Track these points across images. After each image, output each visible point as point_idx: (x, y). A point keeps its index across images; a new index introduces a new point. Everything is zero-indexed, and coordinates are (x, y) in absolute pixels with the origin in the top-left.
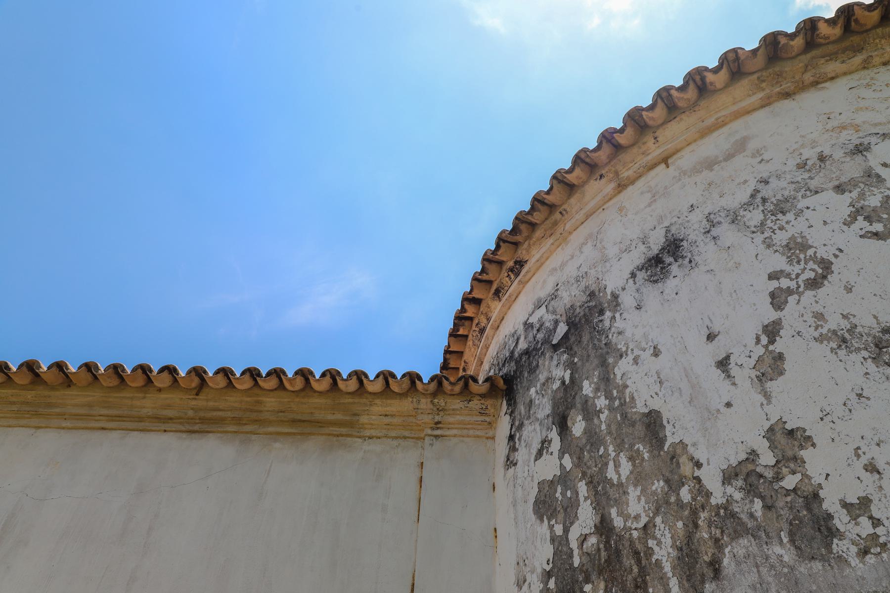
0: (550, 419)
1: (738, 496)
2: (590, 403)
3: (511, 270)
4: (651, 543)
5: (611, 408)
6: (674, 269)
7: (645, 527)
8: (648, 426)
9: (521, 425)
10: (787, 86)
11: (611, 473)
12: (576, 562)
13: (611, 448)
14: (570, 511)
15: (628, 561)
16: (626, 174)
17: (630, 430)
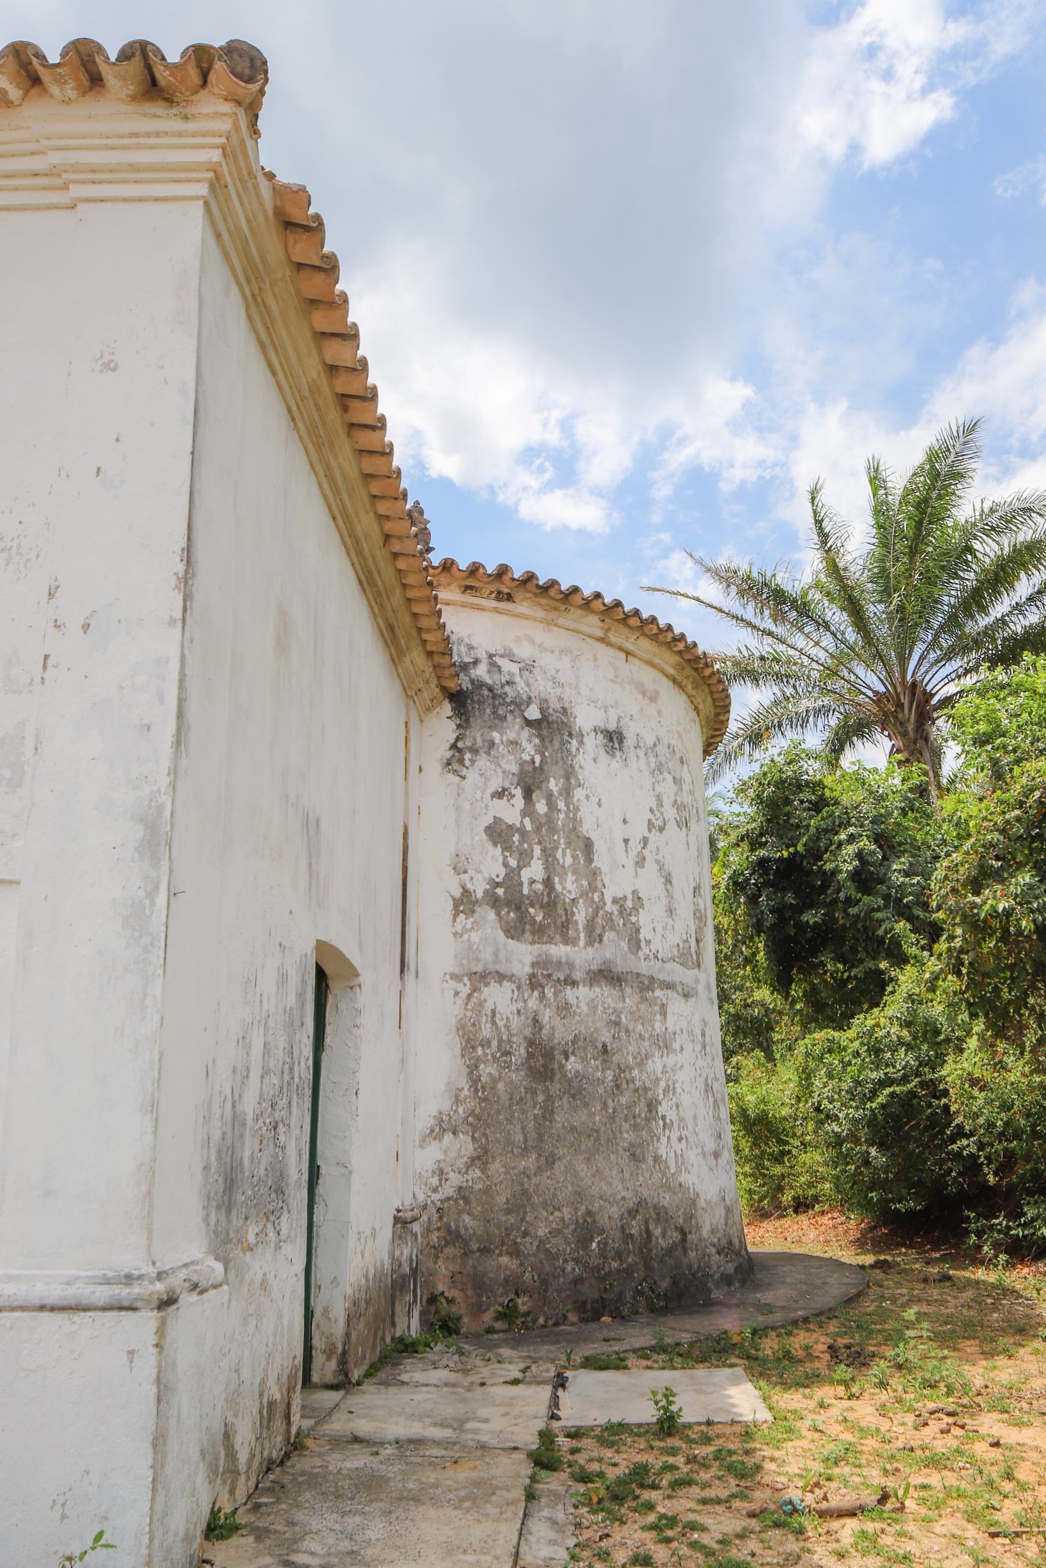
0: (515, 779)
1: (616, 913)
2: (554, 798)
6: (618, 753)
7: (573, 900)
8: (586, 846)
10: (679, 678)
11: (559, 854)
12: (526, 891)
13: (562, 841)
14: (524, 858)
15: (561, 912)
17: (576, 839)
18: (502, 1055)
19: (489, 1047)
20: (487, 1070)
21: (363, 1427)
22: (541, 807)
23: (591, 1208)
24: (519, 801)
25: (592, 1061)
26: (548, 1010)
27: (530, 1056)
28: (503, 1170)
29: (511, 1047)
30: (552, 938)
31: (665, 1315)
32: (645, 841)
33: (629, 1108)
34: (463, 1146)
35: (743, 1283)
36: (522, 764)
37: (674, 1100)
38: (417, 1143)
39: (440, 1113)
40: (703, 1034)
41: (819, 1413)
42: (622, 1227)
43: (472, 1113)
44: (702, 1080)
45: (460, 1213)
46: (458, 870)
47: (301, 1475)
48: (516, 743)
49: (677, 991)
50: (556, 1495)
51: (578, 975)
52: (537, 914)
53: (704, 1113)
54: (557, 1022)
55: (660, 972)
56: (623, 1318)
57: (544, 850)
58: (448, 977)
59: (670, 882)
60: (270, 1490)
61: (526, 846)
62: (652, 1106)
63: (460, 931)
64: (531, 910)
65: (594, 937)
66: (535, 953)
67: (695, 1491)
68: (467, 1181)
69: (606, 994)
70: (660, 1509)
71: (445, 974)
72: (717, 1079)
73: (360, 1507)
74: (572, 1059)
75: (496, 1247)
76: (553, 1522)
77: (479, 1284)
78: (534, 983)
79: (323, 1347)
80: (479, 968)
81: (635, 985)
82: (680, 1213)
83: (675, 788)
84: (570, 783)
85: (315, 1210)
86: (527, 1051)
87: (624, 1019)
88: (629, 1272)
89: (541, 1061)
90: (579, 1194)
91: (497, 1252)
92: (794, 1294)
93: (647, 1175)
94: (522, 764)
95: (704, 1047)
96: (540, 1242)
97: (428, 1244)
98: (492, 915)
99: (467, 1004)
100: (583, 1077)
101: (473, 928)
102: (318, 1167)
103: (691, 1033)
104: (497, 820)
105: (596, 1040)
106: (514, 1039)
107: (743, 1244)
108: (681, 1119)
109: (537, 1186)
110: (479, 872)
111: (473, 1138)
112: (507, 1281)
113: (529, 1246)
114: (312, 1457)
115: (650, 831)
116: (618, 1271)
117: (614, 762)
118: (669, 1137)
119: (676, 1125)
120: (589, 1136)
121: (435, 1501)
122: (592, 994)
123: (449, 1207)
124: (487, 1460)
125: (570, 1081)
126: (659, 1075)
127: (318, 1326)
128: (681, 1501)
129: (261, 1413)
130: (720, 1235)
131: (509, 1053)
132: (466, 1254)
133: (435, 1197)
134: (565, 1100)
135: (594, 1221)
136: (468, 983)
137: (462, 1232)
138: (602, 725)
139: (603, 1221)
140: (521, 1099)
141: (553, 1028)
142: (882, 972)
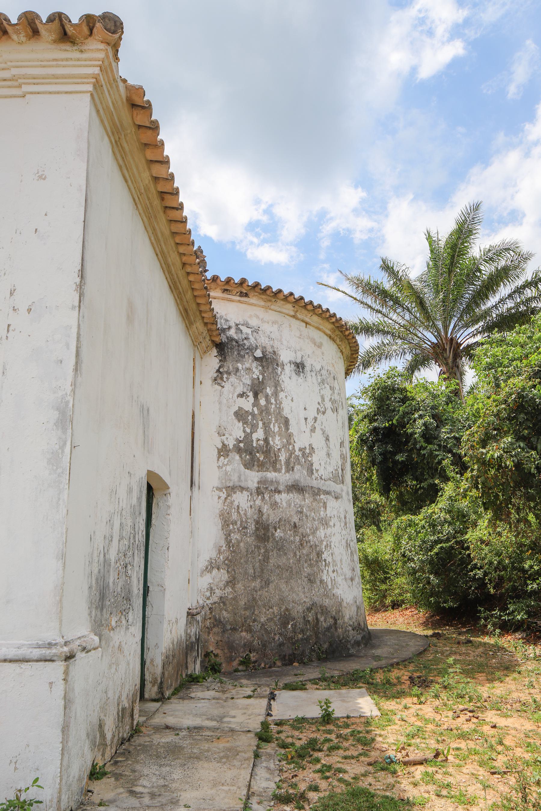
0: (249, 388)
1: (301, 455)
2: (269, 397)
3: (241, 292)
4: (280, 454)
5: (276, 406)
6: (302, 374)
8: (286, 421)
9: (229, 373)
10: (333, 336)
11: (272, 426)
12: (255, 445)
13: (273, 419)
14: (254, 428)
15: (273, 455)
16: (299, 315)
18: (243, 529)
19: (236, 525)
20: (235, 537)
21: (171, 721)
22: (263, 402)
23: (288, 607)
24: (251, 399)
25: (289, 532)
26: (266, 506)
27: (257, 529)
28: (243, 588)
29: (247, 525)
30: (268, 469)
31: (326, 662)
32: (315, 419)
33: (307, 555)
34: (222, 576)
35: (366, 645)
36: (253, 380)
37: (331, 551)
38: (199, 574)
39: (211, 559)
40: (345, 518)
41: (404, 711)
42: (304, 617)
43: (227, 559)
44: (345, 541)
45: (221, 610)
46: (220, 434)
47: (139, 746)
48: (250, 369)
49: (332, 495)
50: (270, 756)
51: (281, 488)
52: (260, 456)
53: (346, 558)
54: (271, 512)
55: (323, 486)
56: (304, 663)
57: (264, 424)
58: (215, 489)
59: (328, 440)
60: (123, 754)
61: (255, 422)
62: (319, 554)
63: (221, 465)
64: (258, 455)
65: (290, 468)
66: (260, 477)
67: (341, 752)
68: (225, 594)
69: (295, 497)
70: (323, 762)
71: (214, 487)
72: (352, 541)
73: (169, 762)
74: (278, 530)
75: (239, 628)
76: (268, 769)
77: (231, 647)
78: (259, 492)
79: (151, 680)
80: (231, 484)
81: (310, 492)
82: (334, 609)
83: (331, 392)
84: (277, 390)
85: (147, 609)
86: (256, 527)
87: (305, 510)
88: (307, 640)
89: (263, 532)
90: (282, 600)
91: (240, 630)
92: (392, 650)
93: (317, 590)
94: (253, 380)
95: (346, 524)
96: (262, 624)
97: (205, 626)
98: (237, 457)
99: (224, 503)
100: (284, 540)
101: (228, 464)
102: (148, 587)
103: (339, 517)
104: (240, 409)
105: (291, 521)
106: (249, 521)
107: (366, 625)
108: (334, 561)
109: (260, 596)
110: (231, 435)
111: (228, 572)
112: (245, 645)
113: (256, 627)
114: (144, 736)
115: (318, 414)
116: (302, 639)
117: (299, 379)
118: (328, 570)
119: (331, 564)
120: (287, 570)
121: (208, 759)
122: (288, 497)
123: (215, 608)
124: (234, 737)
125: (277, 542)
126: (323, 539)
127: (148, 669)
128: (334, 757)
129: (118, 714)
130: (354, 620)
131: (246, 528)
132: (224, 631)
133: (208, 602)
134: (275, 552)
135: (290, 614)
136: (225, 492)
137: (222, 620)
138: (293, 360)
139: (294, 614)
140: (252, 551)
141: (268, 515)
142: (436, 485)
